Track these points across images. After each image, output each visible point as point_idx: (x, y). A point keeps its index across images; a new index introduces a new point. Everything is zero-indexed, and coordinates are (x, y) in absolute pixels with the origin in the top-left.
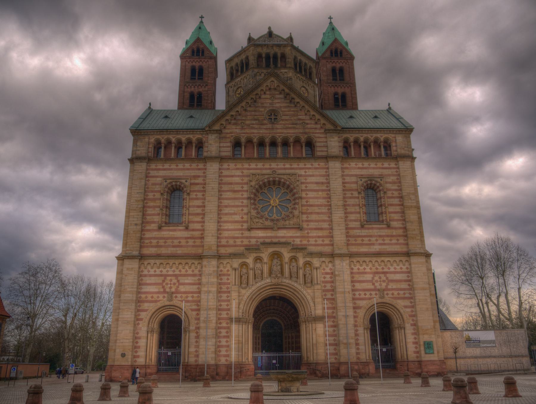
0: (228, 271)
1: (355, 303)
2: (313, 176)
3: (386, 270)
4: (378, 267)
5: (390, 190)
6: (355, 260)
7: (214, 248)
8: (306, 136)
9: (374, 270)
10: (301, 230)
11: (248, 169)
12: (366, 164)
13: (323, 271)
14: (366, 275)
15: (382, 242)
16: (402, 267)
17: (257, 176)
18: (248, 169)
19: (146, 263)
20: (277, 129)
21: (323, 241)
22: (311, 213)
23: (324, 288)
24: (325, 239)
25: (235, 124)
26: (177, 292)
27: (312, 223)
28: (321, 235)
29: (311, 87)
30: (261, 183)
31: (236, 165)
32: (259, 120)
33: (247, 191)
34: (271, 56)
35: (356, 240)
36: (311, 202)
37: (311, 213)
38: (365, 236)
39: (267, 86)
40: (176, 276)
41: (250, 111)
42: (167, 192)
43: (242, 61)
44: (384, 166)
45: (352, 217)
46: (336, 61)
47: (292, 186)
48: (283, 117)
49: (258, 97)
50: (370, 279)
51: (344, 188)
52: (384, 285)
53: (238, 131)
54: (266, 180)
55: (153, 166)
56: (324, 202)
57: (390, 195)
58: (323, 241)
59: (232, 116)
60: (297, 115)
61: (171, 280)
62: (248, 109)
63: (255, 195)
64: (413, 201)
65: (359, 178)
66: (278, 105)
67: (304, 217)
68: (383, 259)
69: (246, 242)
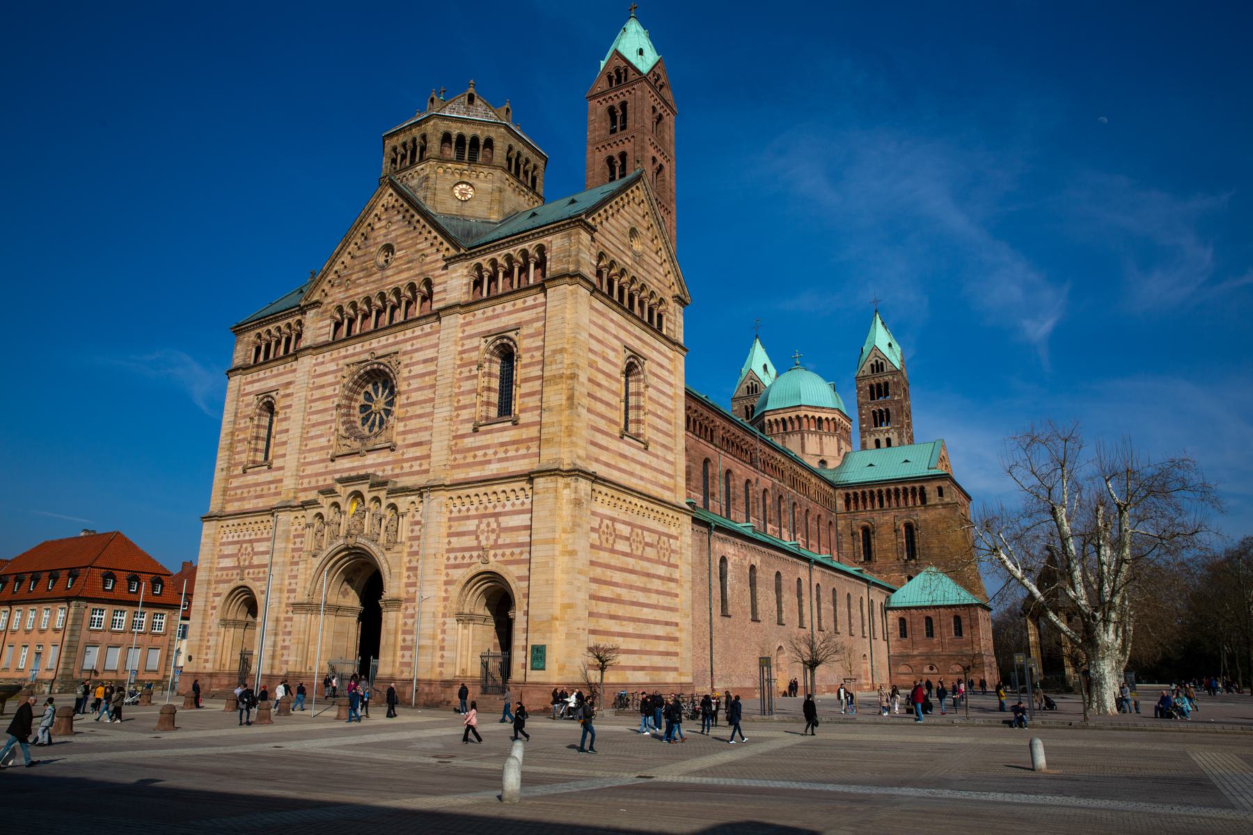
0: (303, 529)
1: (447, 575)
2: (420, 349)
3: (499, 510)
4: (487, 504)
5: (528, 350)
6: (454, 494)
7: (292, 495)
8: (422, 278)
9: (482, 511)
10: (393, 450)
11: (345, 357)
12: (499, 308)
13: (411, 520)
14: (468, 522)
15: (503, 455)
16: (526, 501)
17: (351, 368)
18: (345, 357)
19: (224, 523)
20: (388, 277)
21: (421, 465)
22: (411, 418)
23: (409, 550)
24: (423, 462)
25: (340, 285)
26: (251, 566)
27: (410, 436)
28: (418, 454)
29: (486, 177)
30: (356, 377)
31: (331, 355)
32: (366, 269)
33: (336, 395)
35: (465, 458)
36: (416, 396)
38: (479, 448)
39: (383, 206)
40: (251, 541)
41: (359, 257)
42: (260, 415)
44: (527, 304)
45: (465, 414)
46: (612, 95)
48: (398, 253)
49: (369, 228)
50: (473, 528)
51: (459, 362)
52: (493, 537)
53: (341, 296)
54: (362, 371)
55: (249, 378)
56: (427, 394)
57: (528, 361)
58: (421, 465)
59: (336, 272)
60: (417, 244)
61: (246, 549)
62: (358, 253)
63: (347, 398)
64: (560, 366)
65: (484, 337)
66: (393, 235)
67: (400, 427)
68: (495, 488)
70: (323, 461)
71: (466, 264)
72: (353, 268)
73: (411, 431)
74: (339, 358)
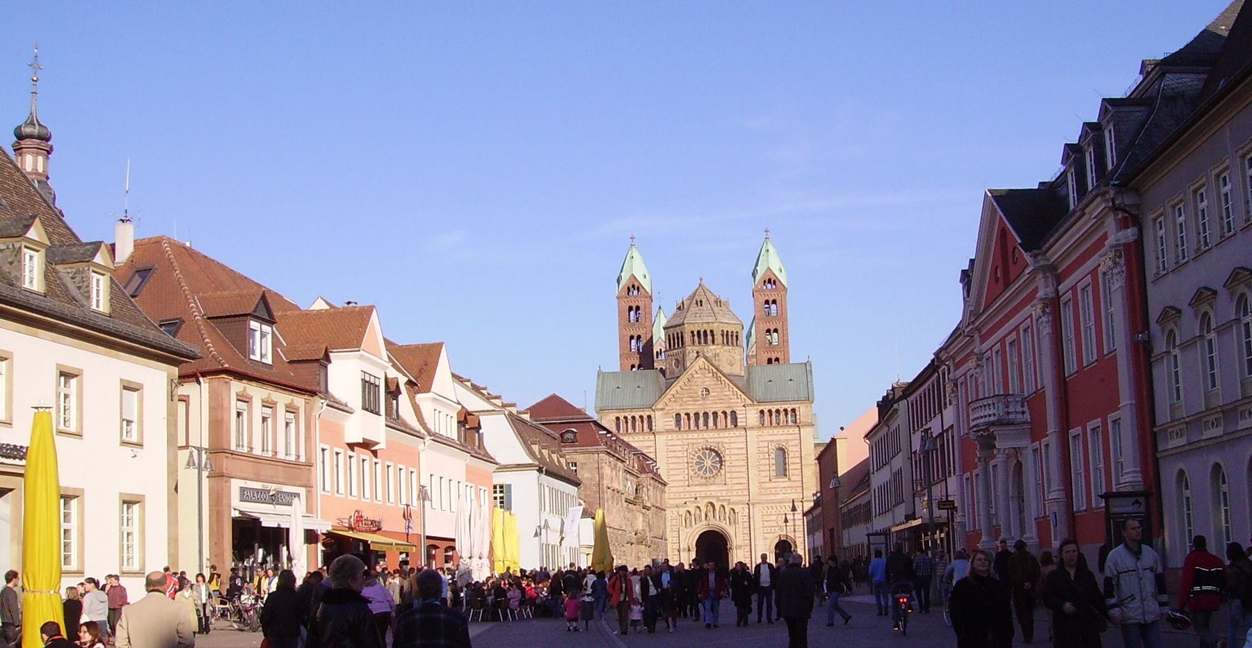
2: (735, 443)
8: (731, 410)
11: (687, 439)
12: (775, 431)
18: (687, 439)
22: (733, 472)
28: (741, 488)
34: (702, 333)
36: (735, 463)
37: (733, 472)
43: (678, 334)
45: (763, 474)
47: (719, 452)
53: (678, 408)
54: (700, 448)
62: (685, 388)
66: (707, 383)
69: (687, 495)
70: (682, 486)
71: (755, 408)
72: (683, 394)
73: (734, 478)
74: (683, 439)
